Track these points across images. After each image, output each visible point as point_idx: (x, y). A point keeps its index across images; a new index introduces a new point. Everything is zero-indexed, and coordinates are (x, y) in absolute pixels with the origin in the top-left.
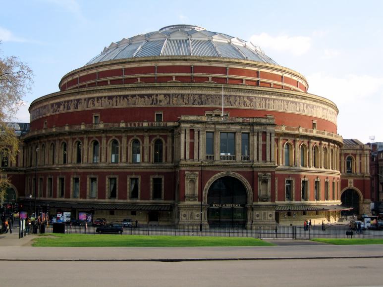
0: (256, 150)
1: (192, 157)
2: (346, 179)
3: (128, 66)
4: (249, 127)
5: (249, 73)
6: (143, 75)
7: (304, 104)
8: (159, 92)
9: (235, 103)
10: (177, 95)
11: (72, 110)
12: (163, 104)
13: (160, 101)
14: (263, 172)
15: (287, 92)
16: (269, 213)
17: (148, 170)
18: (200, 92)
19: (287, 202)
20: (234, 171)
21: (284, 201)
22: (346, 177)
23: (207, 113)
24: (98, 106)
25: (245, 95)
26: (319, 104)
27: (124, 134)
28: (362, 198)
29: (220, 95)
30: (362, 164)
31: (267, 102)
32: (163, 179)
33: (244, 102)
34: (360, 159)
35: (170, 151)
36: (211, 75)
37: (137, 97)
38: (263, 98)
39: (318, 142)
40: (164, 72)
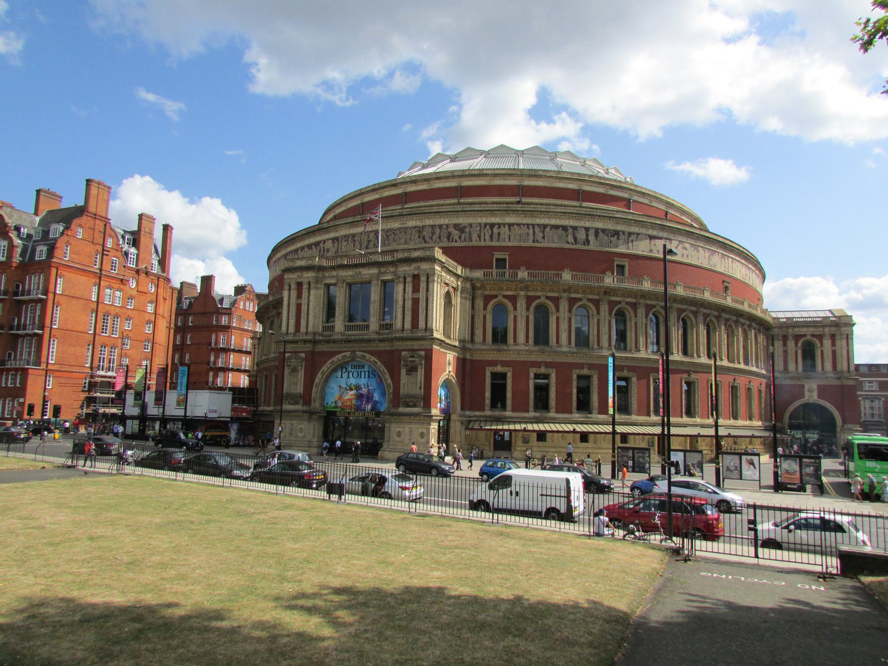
0: (400, 311)
2: (799, 383)
4: (392, 269)
5: (501, 191)
7: (587, 229)
8: (327, 236)
9: (431, 238)
10: (346, 237)
14: (409, 350)
16: (421, 430)
20: (363, 351)
21: (528, 411)
22: (799, 378)
25: (451, 222)
28: (839, 422)
29: (406, 228)
30: (838, 352)
31: (495, 230)
33: (449, 234)
34: (833, 344)
38: (486, 225)
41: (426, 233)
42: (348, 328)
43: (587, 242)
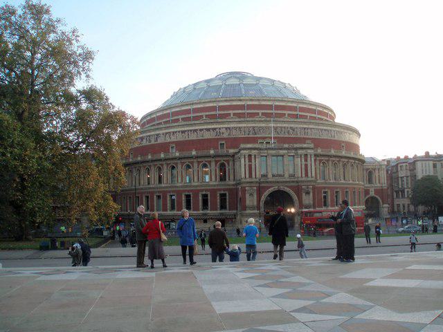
0: (300, 169)
1: (250, 176)
3: (195, 107)
5: (291, 108)
6: (207, 114)
8: (221, 126)
11: (153, 142)
12: (225, 136)
13: (223, 133)
15: (321, 122)
17: (215, 188)
18: (254, 125)
19: (324, 208)
23: (260, 141)
24: (173, 139)
26: (346, 131)
27: (195, 160)
32: (227, 194)
35: (231, 172)
36: (260, 112)
37: (204, 130)
39: (346, 160)
40: (224, 110)
41: (279, 130)
42: (273, 176)
43: (334, 137)
